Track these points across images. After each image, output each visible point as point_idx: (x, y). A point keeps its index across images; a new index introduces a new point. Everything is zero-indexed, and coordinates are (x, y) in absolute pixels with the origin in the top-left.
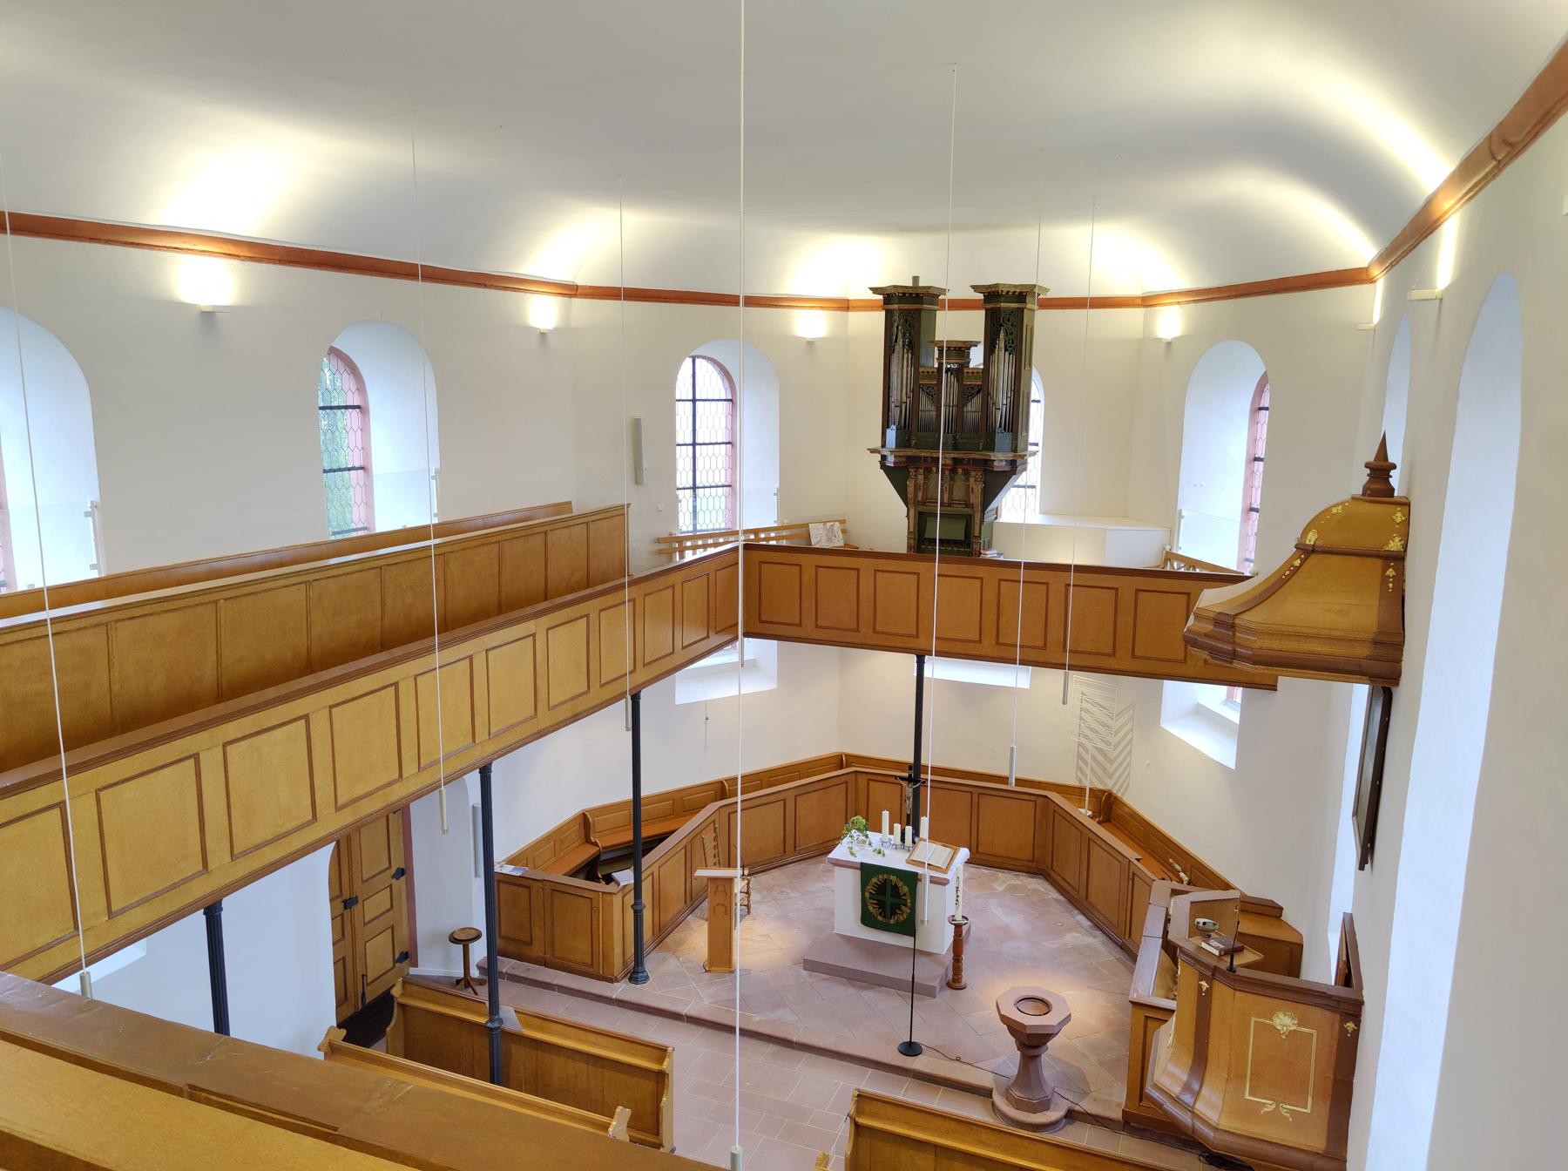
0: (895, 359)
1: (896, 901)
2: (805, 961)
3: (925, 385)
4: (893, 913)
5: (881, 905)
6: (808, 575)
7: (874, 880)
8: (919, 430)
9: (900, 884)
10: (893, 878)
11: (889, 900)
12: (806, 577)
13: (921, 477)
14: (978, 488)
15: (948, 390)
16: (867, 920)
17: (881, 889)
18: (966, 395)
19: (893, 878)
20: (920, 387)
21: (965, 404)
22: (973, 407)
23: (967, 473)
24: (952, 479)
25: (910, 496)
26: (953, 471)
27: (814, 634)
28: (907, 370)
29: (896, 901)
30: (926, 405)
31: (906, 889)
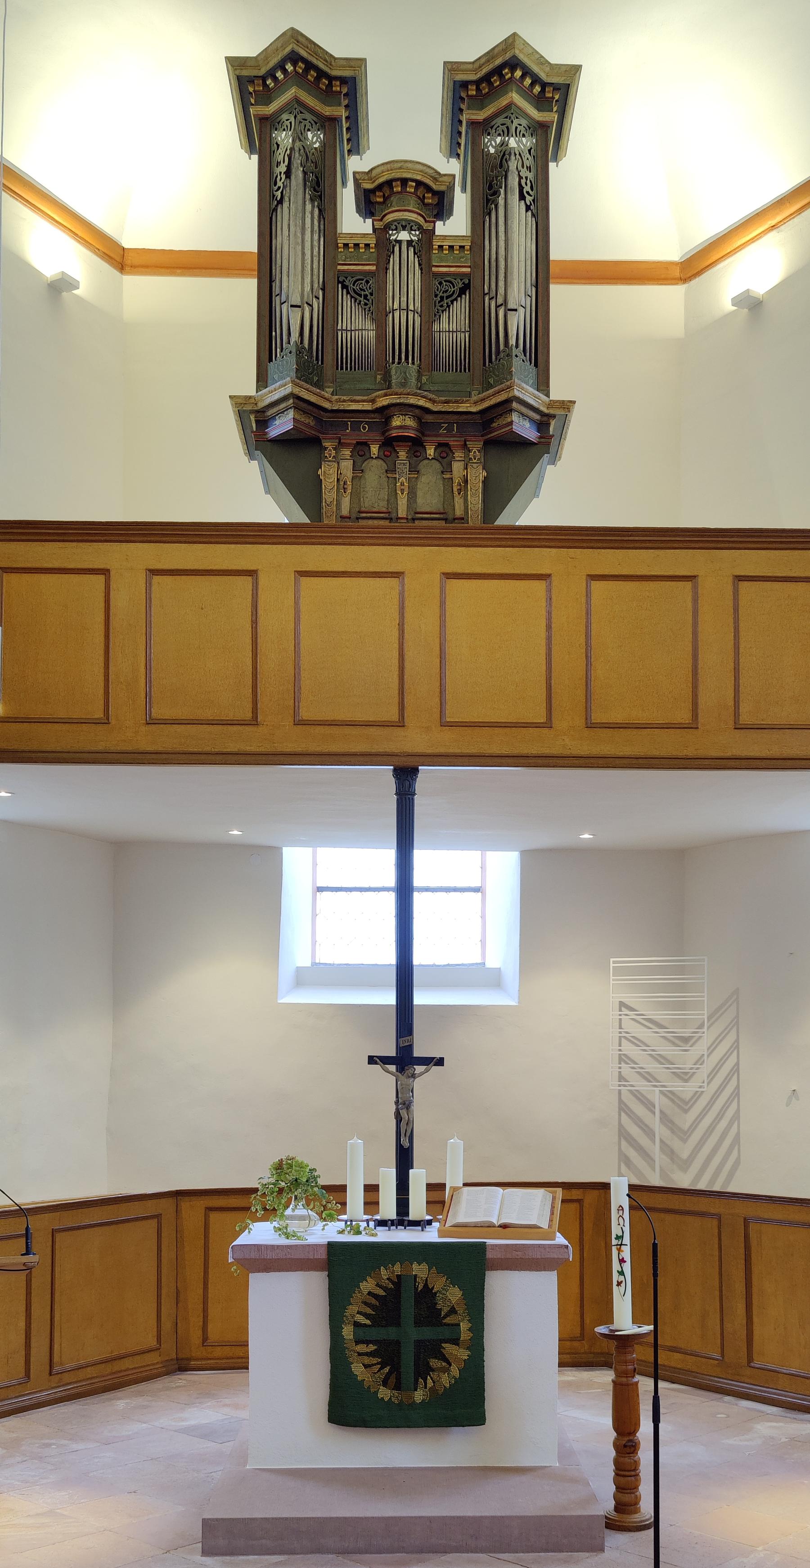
0: (286, 216)
1: (428, 1333)
2: (209, 1526)
3: (352, 279)
4: (422, 1371)
5: (388, 1355)
6: (127, 594)
7: (368, 1285)
8: (339, 365)
9: (438, 1283)
10: (420, 1270)
11: (411, 1333)
12: (119, 600)
13: (347, 465)
14: (477, 475)
15: (405, 287)
16: (348, 1408)
17: (386, 1308)
18: (441, 292)
19: (420, 1270)
20: (343, 281)
21: (437, 316)
22: (454, 324)
23: (444, 450)
24: (414, 469)
25: (329, 495)
26: (416, 445)
27: (145, 740)
28: (312, 243)
29: (428, 1333)
30: (355, 325)
31: (454, 1295)
